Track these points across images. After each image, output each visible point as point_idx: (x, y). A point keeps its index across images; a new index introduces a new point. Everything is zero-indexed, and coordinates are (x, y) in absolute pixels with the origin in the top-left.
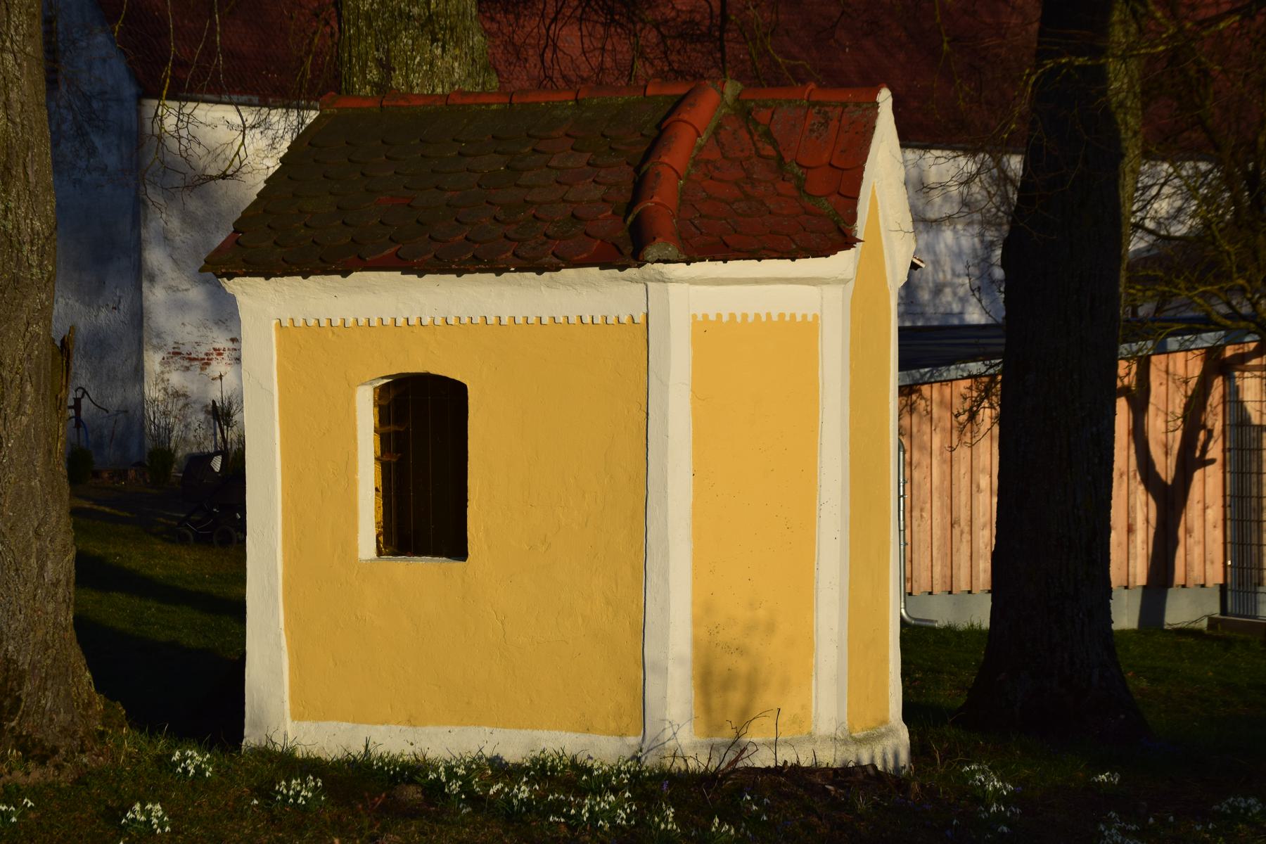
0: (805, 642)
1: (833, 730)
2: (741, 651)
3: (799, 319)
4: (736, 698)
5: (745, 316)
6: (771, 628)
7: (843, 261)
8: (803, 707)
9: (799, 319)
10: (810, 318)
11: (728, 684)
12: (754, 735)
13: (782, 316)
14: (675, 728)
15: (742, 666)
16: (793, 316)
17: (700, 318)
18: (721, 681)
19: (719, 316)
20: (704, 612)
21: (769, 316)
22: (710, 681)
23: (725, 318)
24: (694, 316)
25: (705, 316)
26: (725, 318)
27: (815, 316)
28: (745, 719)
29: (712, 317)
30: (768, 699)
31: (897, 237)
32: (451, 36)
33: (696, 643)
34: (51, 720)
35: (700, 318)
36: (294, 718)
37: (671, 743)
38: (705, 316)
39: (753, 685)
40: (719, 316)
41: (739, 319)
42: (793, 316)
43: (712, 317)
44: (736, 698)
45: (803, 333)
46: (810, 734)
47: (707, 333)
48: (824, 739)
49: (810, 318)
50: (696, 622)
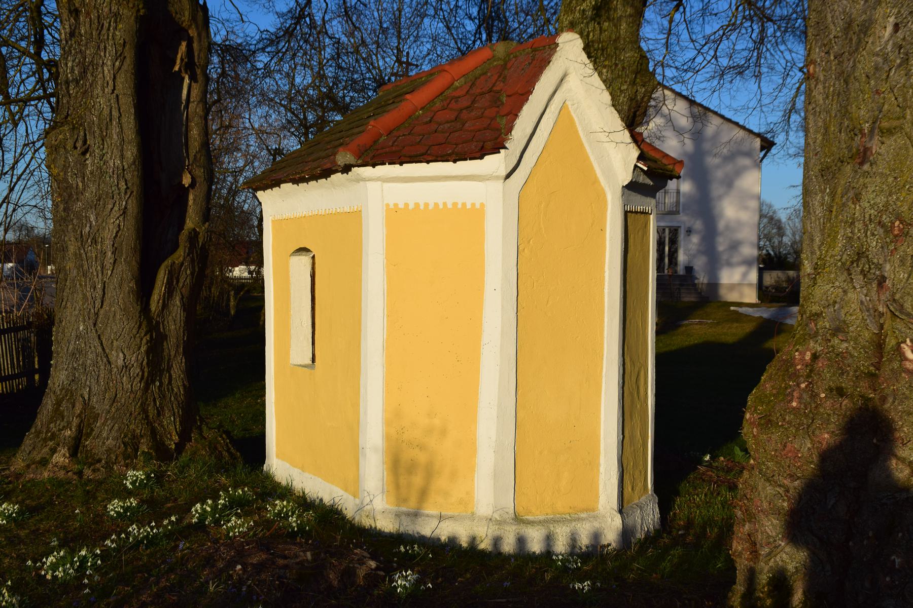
0: (470, 446)
1: (491, 513)
2: (422, 447)
3: (469, 206)
4: (418, 480)
5: (426, 205)
6: (444, 432)
7: (495, 163)
8: (467, 493)
9: (469, 206)
10: (478, 206)
11: (412, 468)
12: (430, 509)
13: (455, 204)
14: (372, 497)
15: (422, 458)
16: (464, 205)
17: (392, 206)
18: (406, 468)
19: (407, 205)
20: (394, 417)
21: (445, 204)
22: (399, 466)
23: (411, 206)
24: (388, 205)
25: (396, 205)
26: (411, 206)
27: (482, 205)
28: (423, 494)
29: (401, 206)
30: (440, 483)
31: (610, 148)
32: (602, 54)
33: (387, 438)
34: (104, 443)
35: (392, 206)
36: (277, 456)
37: (368, 507)
38: (396, 205)
39: (430, 473)
40: (407, 205)
41: (422, 207)
42: (464, 205)
43: (401, 206)
44: (418, 480)
45: (474, 216)
46: (473, 514)
47: (395, 216)
48: (481, 519)
49: (478, 206)
50: (388, 423)
